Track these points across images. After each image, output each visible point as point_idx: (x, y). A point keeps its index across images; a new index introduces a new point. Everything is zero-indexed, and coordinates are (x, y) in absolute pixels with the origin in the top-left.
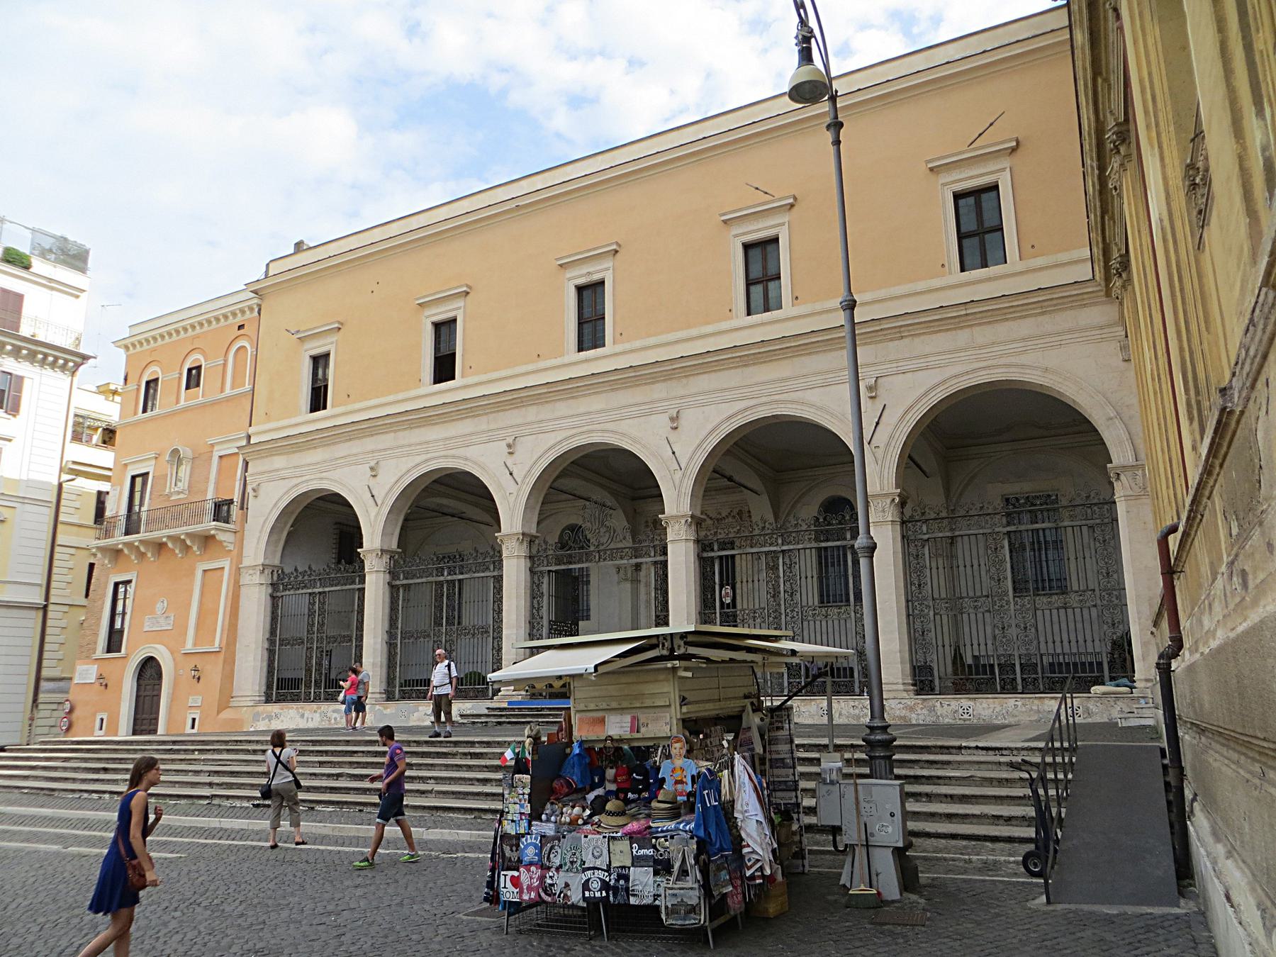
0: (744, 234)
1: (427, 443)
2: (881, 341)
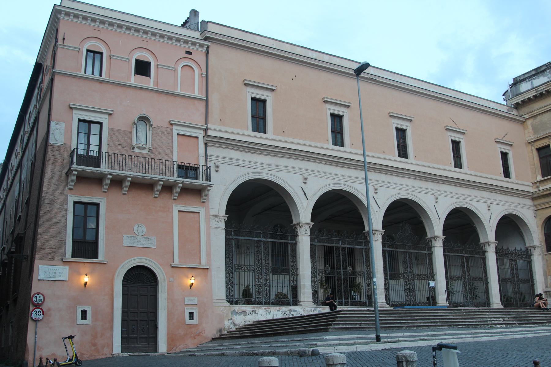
2: (490, 192)
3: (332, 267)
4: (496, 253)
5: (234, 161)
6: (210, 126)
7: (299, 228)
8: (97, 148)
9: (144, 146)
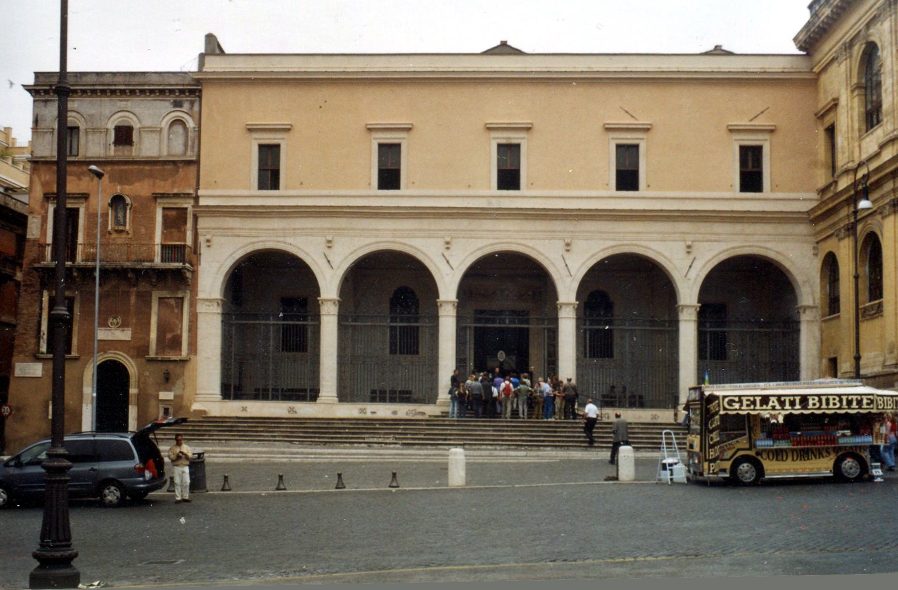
0: (618, 139)
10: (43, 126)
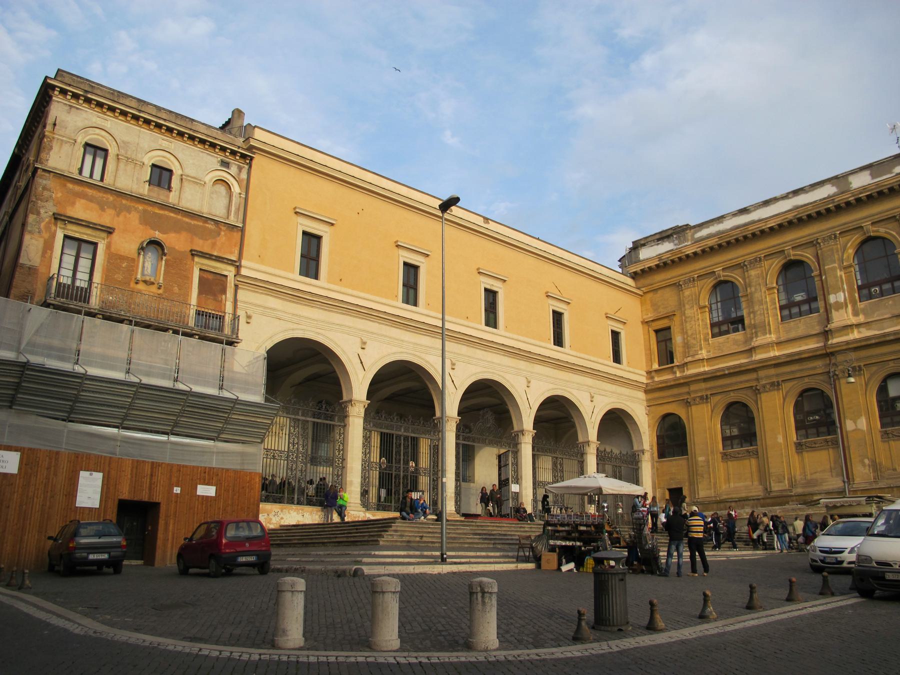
1: (403, 341)
2: (595, 379)
3: (389, 460)
4: (597, 456)
5: (272, 312)
6: (244, 263)
7: (350, 407)
8: (87, 277)
9: (152, 280)
10: (61, 132)
